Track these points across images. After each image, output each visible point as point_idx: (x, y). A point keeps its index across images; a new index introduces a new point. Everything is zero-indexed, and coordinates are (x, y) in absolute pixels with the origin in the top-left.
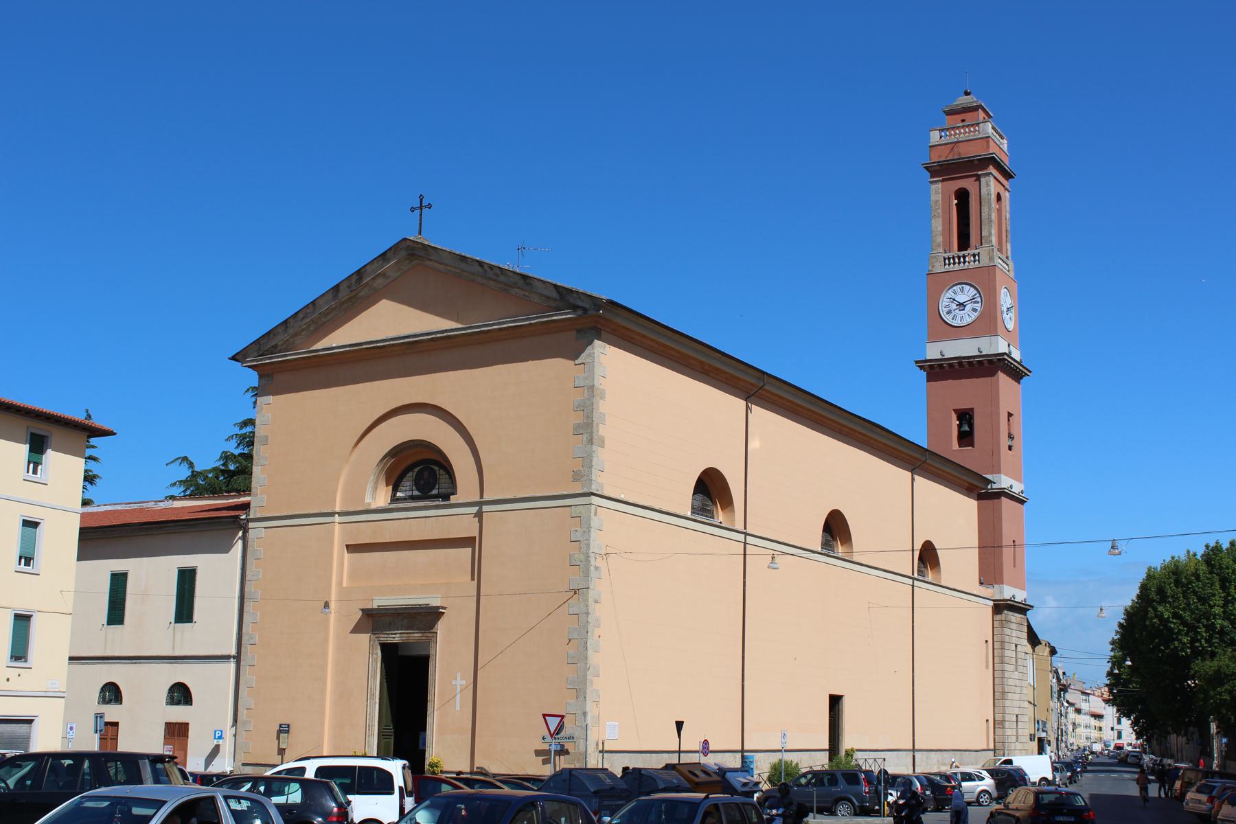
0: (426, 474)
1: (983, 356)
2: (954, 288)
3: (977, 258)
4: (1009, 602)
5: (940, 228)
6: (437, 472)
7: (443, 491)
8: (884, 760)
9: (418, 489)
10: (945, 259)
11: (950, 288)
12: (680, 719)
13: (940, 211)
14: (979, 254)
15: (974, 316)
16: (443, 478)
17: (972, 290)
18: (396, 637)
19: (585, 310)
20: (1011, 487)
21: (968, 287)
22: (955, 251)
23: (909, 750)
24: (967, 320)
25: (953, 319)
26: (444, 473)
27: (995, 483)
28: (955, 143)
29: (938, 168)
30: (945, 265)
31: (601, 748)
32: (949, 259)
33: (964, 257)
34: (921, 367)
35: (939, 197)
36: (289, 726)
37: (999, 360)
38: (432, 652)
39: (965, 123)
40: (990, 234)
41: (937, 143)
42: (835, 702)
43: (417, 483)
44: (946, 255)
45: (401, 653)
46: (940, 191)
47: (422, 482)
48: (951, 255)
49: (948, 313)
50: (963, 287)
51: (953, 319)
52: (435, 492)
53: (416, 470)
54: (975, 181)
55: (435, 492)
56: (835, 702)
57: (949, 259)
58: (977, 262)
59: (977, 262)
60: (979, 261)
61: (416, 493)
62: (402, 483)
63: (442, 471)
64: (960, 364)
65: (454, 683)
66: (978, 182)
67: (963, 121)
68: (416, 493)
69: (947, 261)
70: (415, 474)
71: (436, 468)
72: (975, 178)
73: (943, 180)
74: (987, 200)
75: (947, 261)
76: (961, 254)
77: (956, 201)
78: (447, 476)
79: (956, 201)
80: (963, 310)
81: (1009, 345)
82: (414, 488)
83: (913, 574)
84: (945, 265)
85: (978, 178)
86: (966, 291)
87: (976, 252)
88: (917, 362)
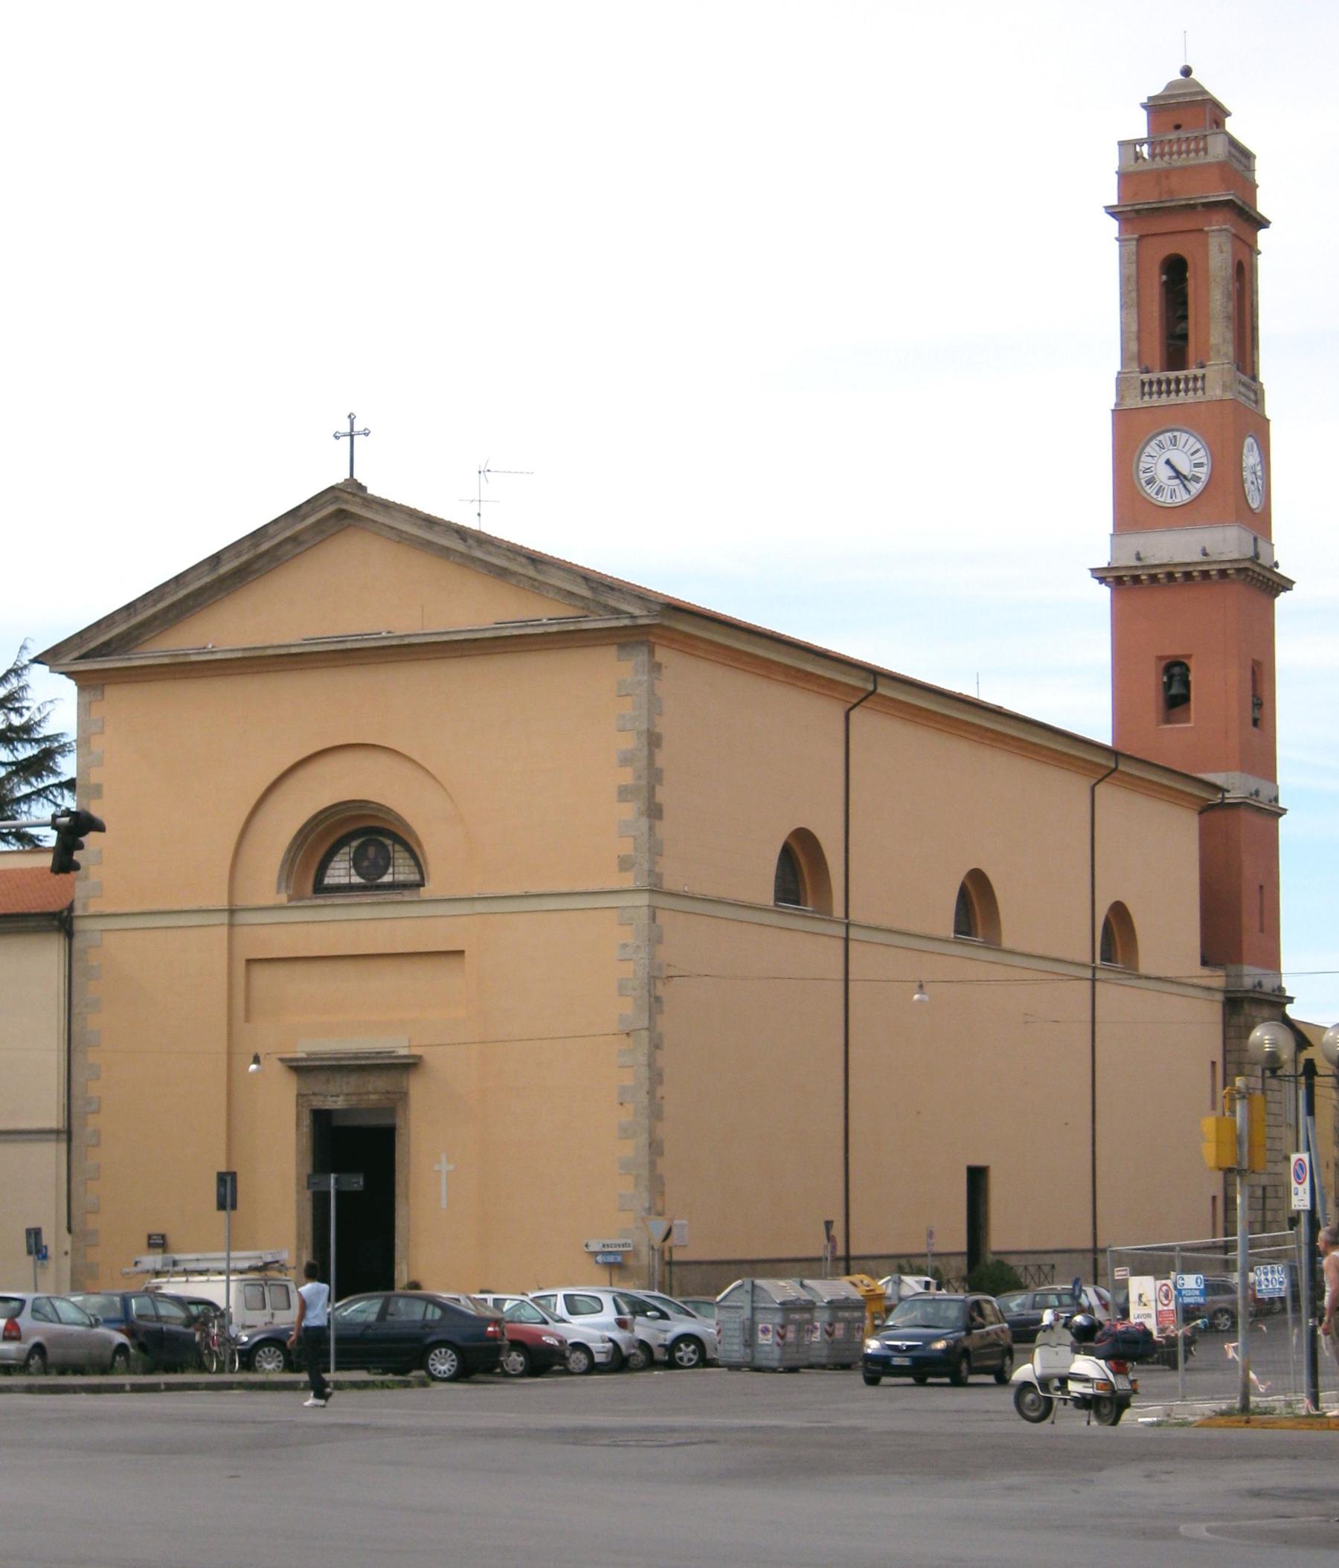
0: (371, 851)
1: (1209, 563)
2: (1161, 438)
4: (1251, 995)
6: (390, 848)
7: (401, 878)
8: (1053, 1267)
9: (359, 874)
10: (1143, 384)
11: (1151, 439)
12: (829, 1219)
14: (1203, 377)
16: (401, 858)
18: (336, 1098)
19: (633, 617)
20: (1257, 793)
23: (1083, 1251)
25: (1157, 494)
26: (402, 849)
27: (1228, 791)
30: (1143, 394)
31: (667, 1257)
32: (1151, 383)
33: (1178, 381)
34: (1102, 580)
36: (163, 1237)
37: (1238, 570)
38: (399, 1122)
39: (1182, 134)
42: (977, 1177)
43: (357, 863)
44: (1146, 377)
45: (338, 1122)
47: (366, 864)
49: (1148, 482)
50: (1175, 437)
51: (1157, 494)
52: (387, 878)
53: (355, 844)
55: (387, 878)
56: (977, 1177)
57: (1151, 383)
58: (1200, 393)
59: (1200, 393)
60: (1203, 389)
61: (356, 880)
62: (333, 864)
63: (398, 847)
64: (1170, 576)
65: (436, 1167)
67: (1178, 127)
68: (356, 880)
69: (1147, 389)
70: (353, 850)
71: (388, 842)
75: (1147, 389)
76: (1172, 375)
78: (407, 855)
81: (1255, 539)
82: (353, 871)
83: (1093, 961)
84: (1143, 394)
86: (1181, 443)
87: (1199, 372)
88: (1093, 570)
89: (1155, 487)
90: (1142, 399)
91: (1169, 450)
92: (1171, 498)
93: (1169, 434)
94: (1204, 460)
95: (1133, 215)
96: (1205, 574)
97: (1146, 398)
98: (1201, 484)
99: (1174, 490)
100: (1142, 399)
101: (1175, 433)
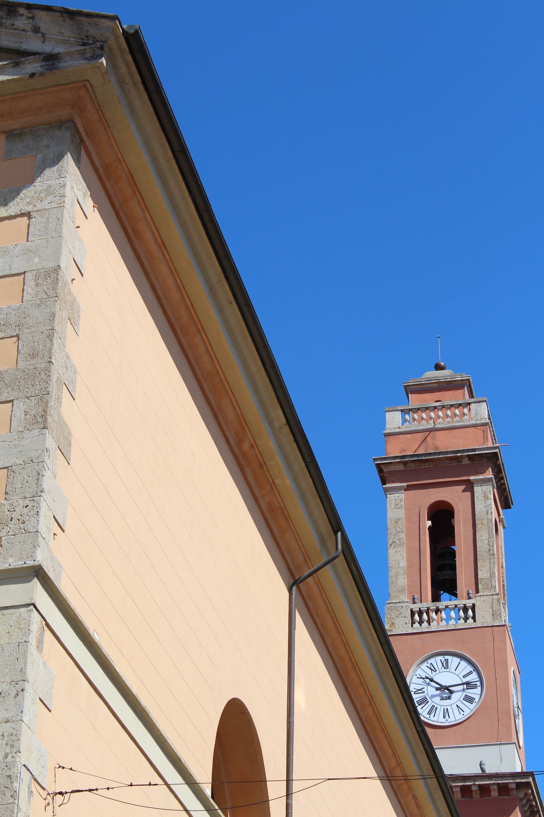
2: (432, 661)
3: (470, 613)
5: (403, 564)
10: (413, 613)
13: (403, 535)
14: (473, 607)
15: (469, 709)
17: (465, 667)
21: (456, 660)
22: (428, 603)
24: (456, 717)
28: (430, 431)
29: (401, 467)
30: (413, 623)
32: (420, 613)
35: (401, 514)
37: (519, 785)
40: (492, 576)
41: (398, 430)
44: (416, 607)
46: (403, 503)
48: (423, 606)
50: (447, 661)
54: (464, 491)
57: (420, 613)
59: (470, 621)
60: (474, 618)
66: (468, 494)
69: (417, 617)
72: (463, 487)
73: (409, 488)
74: (485, 522)
75: (417, 617)
77: (429, 523)
79: (429, 523)
80: (449, 698)
84: (413, 623)
85: (469, 486)
87: (469, 603)
89: (428, 707)
90: (412, 626)
91: (440, 672)
92: (444, 718)
93: (441, 658)
94: (477, 698)
95: (401, 467)
96: (484, 790)
97: (416, 625)
98: (474, 704)
99: (447, 709)
100: (412, 626)
101: (446, 657)
